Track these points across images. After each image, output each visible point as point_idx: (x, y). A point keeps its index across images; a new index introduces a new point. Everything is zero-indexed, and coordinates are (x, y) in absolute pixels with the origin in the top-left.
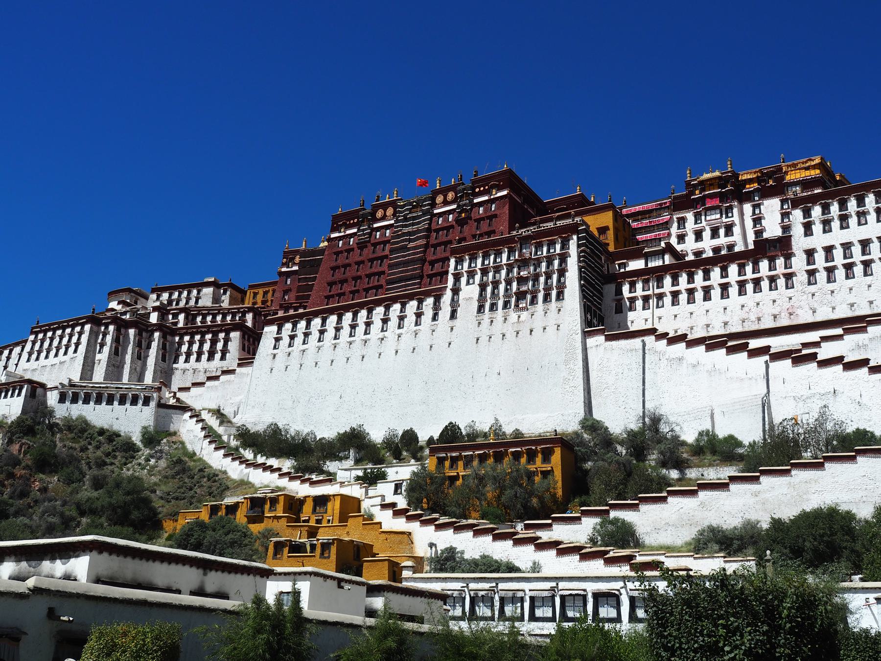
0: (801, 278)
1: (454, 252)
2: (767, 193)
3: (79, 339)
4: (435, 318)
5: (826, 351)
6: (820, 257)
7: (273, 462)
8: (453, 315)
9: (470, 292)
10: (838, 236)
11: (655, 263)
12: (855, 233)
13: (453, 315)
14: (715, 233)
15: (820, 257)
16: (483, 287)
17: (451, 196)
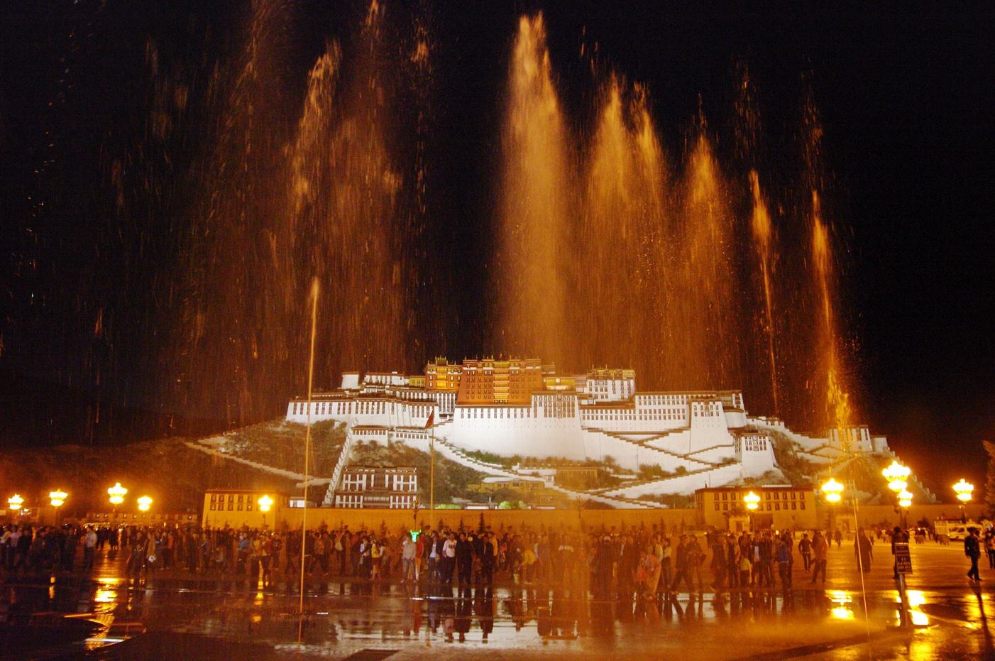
0: (638, 417)
1: (534, 394)
2: (616, 378)
3: (384, 407)
4: (529, 416)
5: (650, 443)
6: (643, 412)
7: (487, 464)
8: (536, 416)
9: (541, 410)
10: (647, 407)
11: (591, 402)
12: (653, 407)
13: (536, 416)
14: (602, 390)
15: (643, 412)
16: (546, 407)
17: (517, 364)
